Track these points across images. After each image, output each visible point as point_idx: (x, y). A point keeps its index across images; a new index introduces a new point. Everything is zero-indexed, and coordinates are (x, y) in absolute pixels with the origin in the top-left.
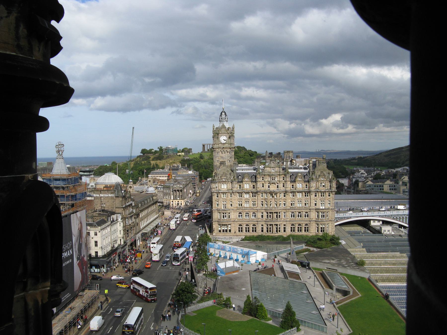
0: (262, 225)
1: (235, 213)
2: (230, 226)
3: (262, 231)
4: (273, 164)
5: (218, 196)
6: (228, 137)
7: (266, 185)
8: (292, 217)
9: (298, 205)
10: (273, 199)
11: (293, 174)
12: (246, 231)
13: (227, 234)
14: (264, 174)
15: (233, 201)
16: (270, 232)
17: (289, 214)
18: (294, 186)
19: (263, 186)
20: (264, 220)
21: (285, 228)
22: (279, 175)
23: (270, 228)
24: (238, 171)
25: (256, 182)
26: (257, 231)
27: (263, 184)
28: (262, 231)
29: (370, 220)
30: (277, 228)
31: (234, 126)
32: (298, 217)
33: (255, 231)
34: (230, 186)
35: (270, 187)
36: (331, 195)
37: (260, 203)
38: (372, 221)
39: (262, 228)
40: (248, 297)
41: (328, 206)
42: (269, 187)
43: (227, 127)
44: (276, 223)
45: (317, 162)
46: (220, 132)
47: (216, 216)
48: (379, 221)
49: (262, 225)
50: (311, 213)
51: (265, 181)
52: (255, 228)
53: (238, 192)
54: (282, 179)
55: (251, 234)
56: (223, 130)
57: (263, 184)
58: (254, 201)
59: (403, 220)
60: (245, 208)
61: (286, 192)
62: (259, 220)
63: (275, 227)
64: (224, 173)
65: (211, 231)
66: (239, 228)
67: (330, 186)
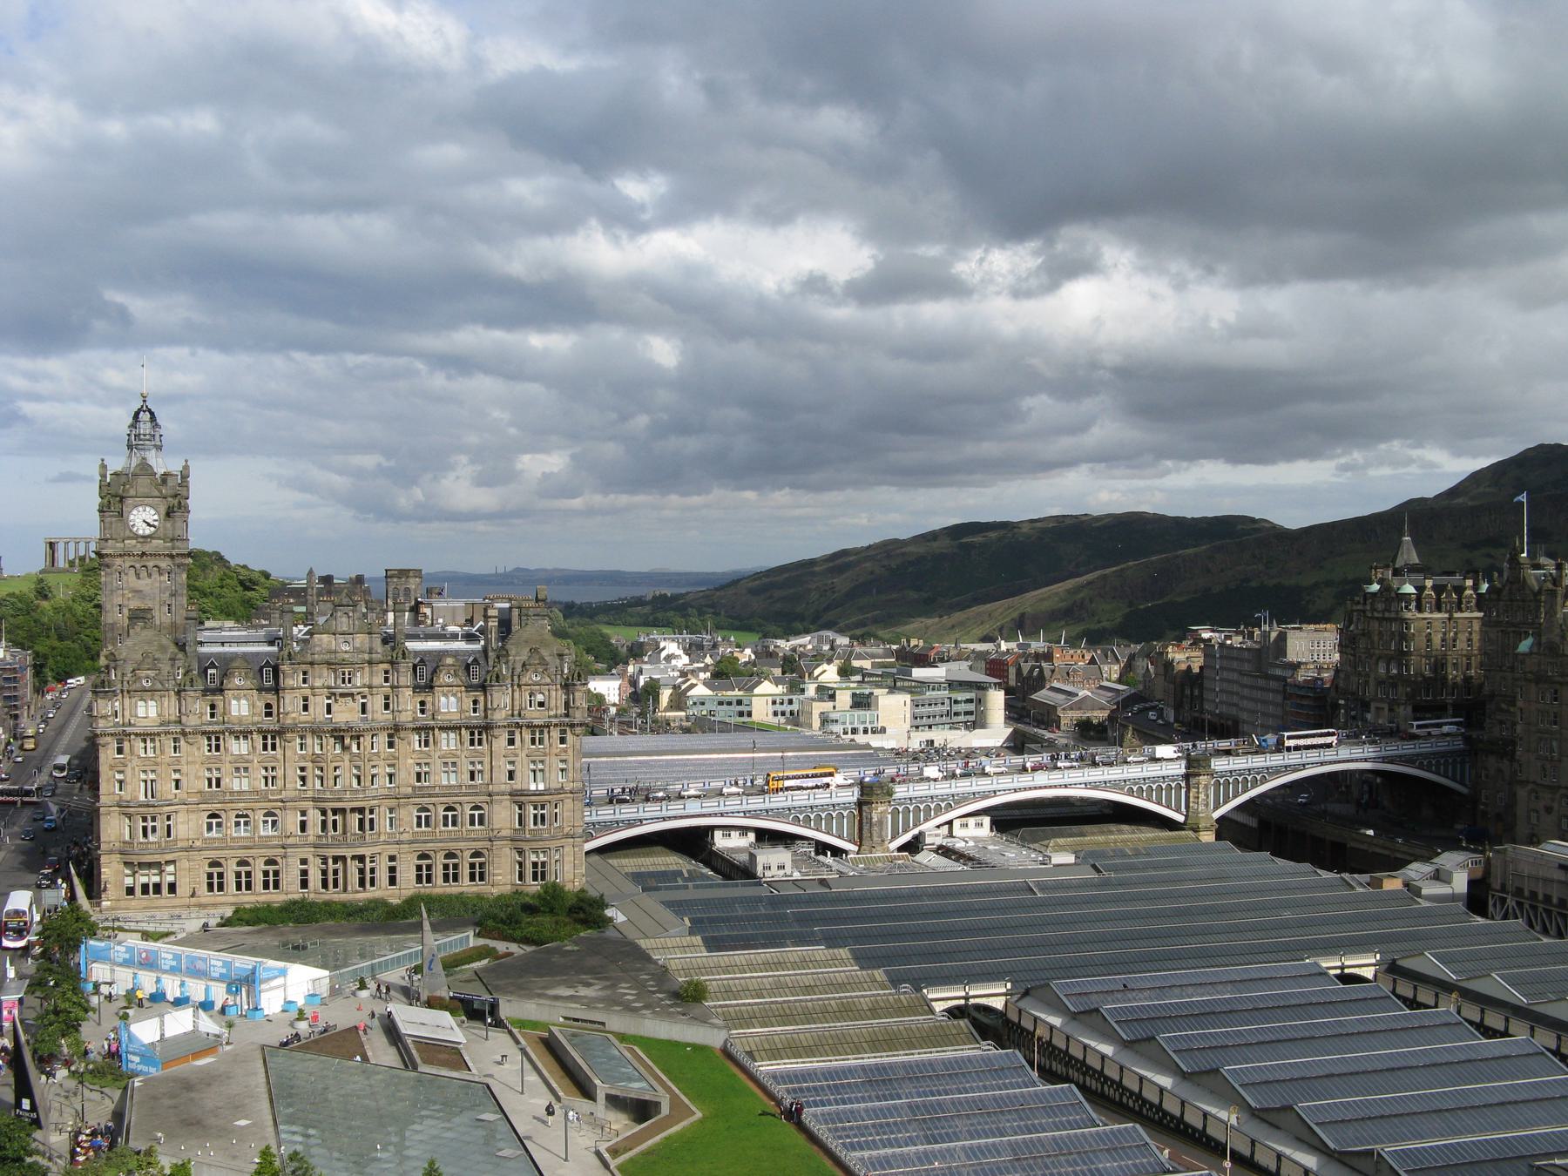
0: (304, 862)
1: (193, 816)
2: (171, 868)
3: (304, 884)
4: (345, 619)
5: (120, 751)
6: (163, 510)
7: (319, 703)
8: (419, 825)
9: (444, 779)
10: (347, 757)
11: (423, 658)
12: (239, 887)
13: (162, 902)
14: (309, 659)
15: (184, 768)
16: (335, 886)
17: (409, 814)
18: (428, 706)
19: (306, 708)
20: (311, 839)
21: (392, 870)
22: (370, 663)
23: (335, 872)
25: (277, 690)
26: (283, 884)
27: (306, 699)
28: (304, 884)
29: (713, 828)
30: (362, 871)
31: (186, 467)
32: (446, 825)
33: (276, 886)
34: (170, 706)
36: (569, 737)
37: (294, 774)
38: (718, 834)
39: (304, 873)
40: (266, 1154)
41: (557, 780)
42: (329, 712)
43: (160, 471)
44: (360, 851)
45: (516, 612)
46: (132, 492)
47: (113, 829)
48: (744, 830)
49: (304, 862)
50: (496, 807)
51: (312, 688)
52: (276, 873)
53: (204, 733)
54: (379, 679)
55: (259, 896)
56: (143, 484)
57: (306, 699)
58: (269, 765)
59: (1438, 768)
60: (232, 793)
61: (395, 732)
62: (290, 841)
63: (353, 867)
64: (145, 655)
65: (94, 889)
66: (210, 876)
67: (567, 705)
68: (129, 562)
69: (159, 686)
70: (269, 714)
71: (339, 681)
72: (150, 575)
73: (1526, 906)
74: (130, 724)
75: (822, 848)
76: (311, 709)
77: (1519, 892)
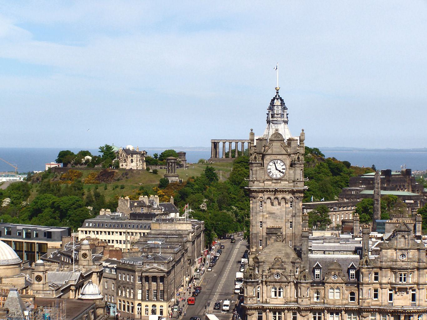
4: (403, 240)
6: (288, 162)
7: (384, 294)
14: (379, 264)
19: (376, 296)
22: (418, 269)
24: (311, 256)
25: (359, 285)
27: (376, 290)
31: (303, 134)
34: (290, 292)
35: (395, 296)
42: (391, 299)
43: (286, 137)
46: (270, 152)
51: (381, 284)
56: (276, 146)
57: (376, 290)
64: (277, 260)
68: (266, 195)
69: (285, 279)
70: (352, 299)
71: (398, 280)
72: (279, 204)
74: (266, 303)
76: (379, 296)
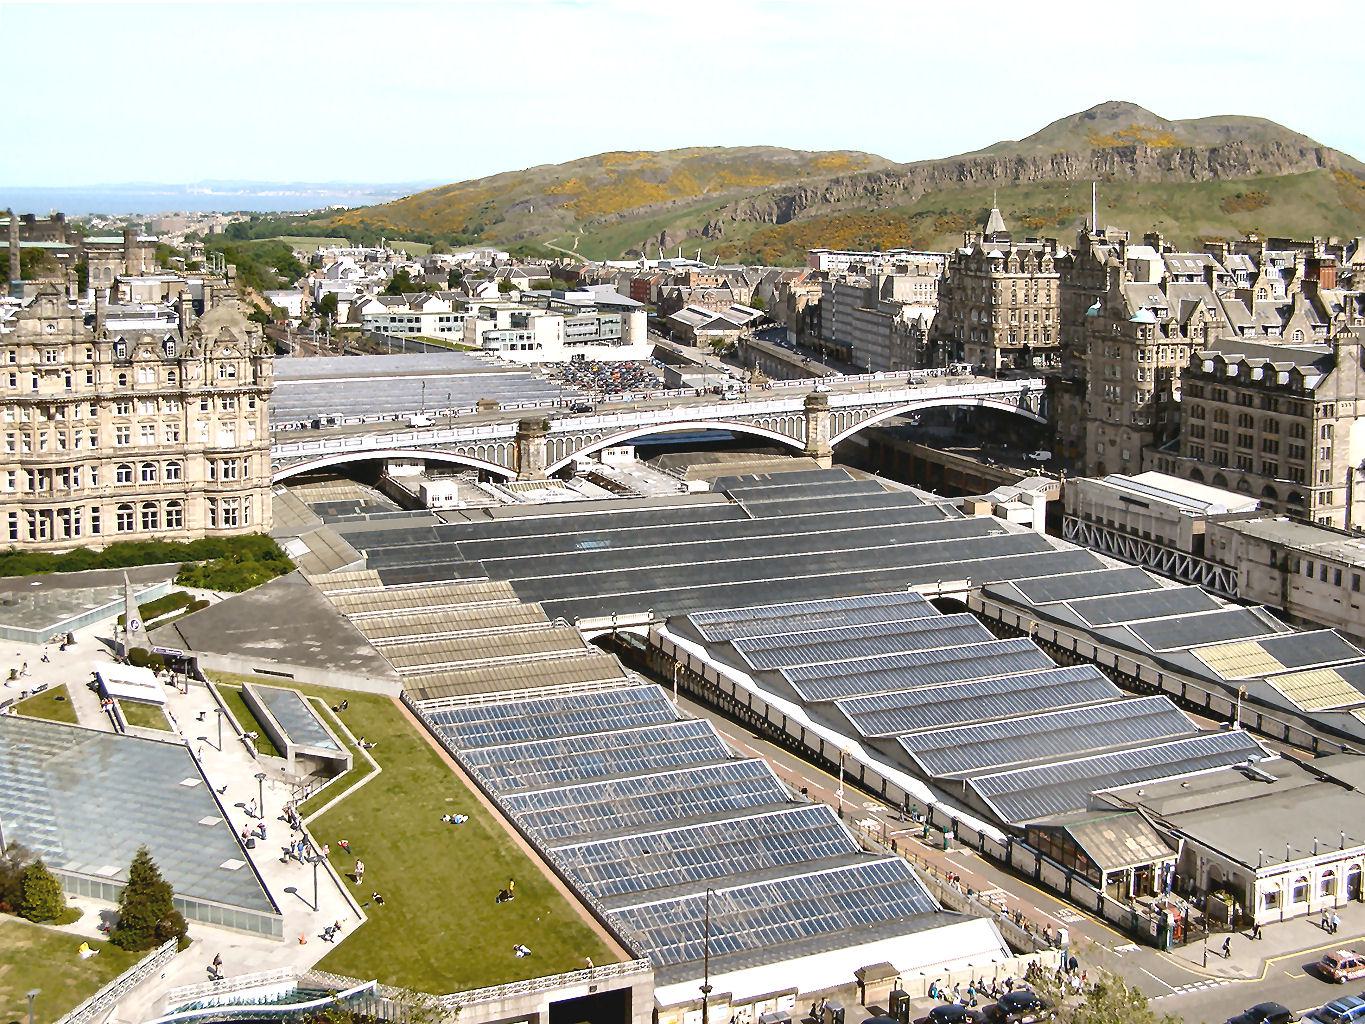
9: (139, 440)
10: (52, 424)
16: (43, 535)
17: (109, 473)
18: (128, 379)
19: (13, 383)
20: (19, 496)
23: (42, 523)
30: (67, 522)
35: (40, 381)
42: (35, 385)
49: (12, 515)
57: (12, 375)
61: (96, 401)
63: (59, 522)
67: (255, 372)
73: (1093, 528)
75: (485, 476)
77: (1088, 517)
